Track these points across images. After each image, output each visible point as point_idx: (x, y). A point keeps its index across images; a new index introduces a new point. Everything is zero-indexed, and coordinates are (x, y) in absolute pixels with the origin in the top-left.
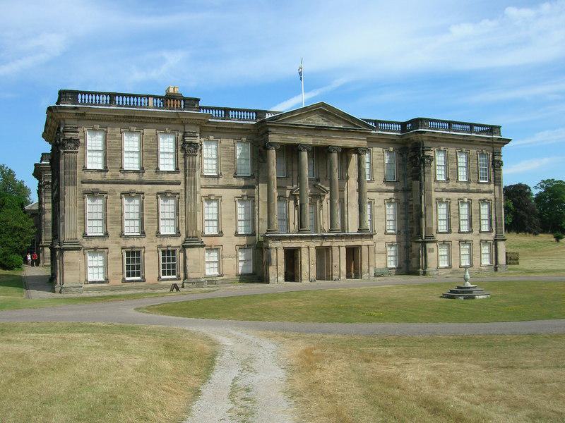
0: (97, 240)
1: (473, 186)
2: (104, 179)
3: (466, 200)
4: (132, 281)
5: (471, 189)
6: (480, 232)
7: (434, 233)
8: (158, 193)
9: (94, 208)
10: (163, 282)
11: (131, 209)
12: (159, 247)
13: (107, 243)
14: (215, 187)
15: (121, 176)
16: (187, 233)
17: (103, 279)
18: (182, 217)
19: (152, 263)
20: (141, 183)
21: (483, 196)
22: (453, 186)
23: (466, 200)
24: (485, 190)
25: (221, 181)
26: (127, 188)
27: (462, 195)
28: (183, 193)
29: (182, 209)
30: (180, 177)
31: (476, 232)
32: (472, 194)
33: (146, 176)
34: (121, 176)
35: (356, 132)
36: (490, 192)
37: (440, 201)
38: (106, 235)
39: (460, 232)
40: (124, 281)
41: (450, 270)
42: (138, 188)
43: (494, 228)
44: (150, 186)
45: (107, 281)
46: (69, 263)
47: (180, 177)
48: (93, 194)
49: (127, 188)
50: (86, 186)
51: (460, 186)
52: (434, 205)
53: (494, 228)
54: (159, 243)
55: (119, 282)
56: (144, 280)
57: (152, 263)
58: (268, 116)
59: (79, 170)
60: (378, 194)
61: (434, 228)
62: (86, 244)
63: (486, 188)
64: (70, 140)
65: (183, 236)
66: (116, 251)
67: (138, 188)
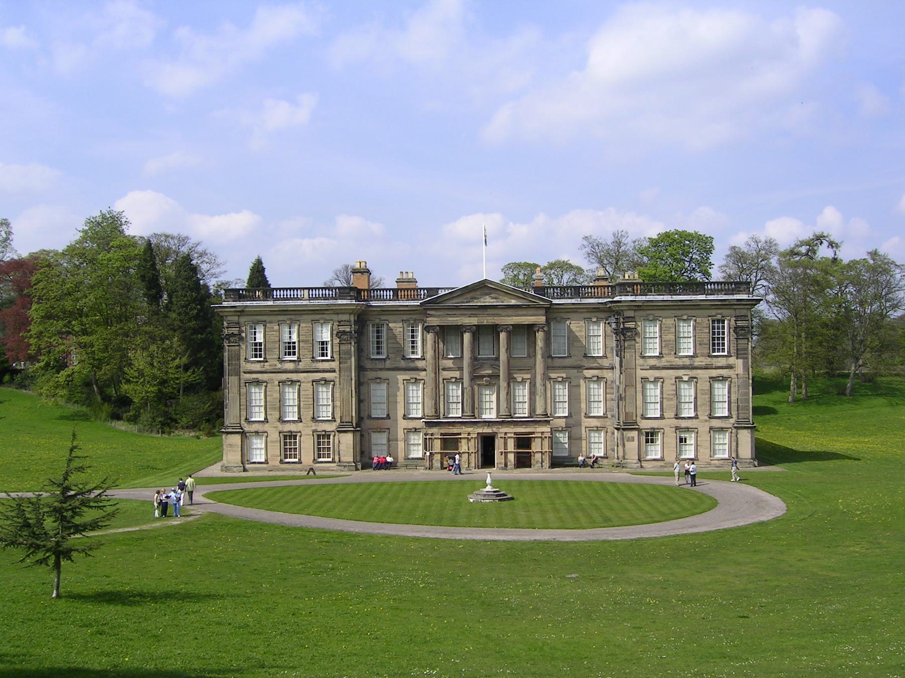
0: (256, 425)
1: (697, 362)
2: (263, 369)
3: (686, 378)
4: (289, 463)
5: (696, 364)
6: (711, 417)
7: (639, 419)
8: (313, 381)
9: (257, 395)
10: (318, 465)
11: (291, 395)
12: (314, 431)
13: (266, 427)
14: (381, 369)
15: (279, 366)
16: (341, 417)
17: (263, 460)
18: (338, 403)
19: (307, 446)
20: (296, 372)
21: (715, 373)
22: (668, 362)
23: (686, 378)
24: (720, 364)
25: (388, 364)
26: (284, 376)
27: (680, 373)
28: (338, 380)
29: (337, 395)
30: (335, 365)
31: (703, 416)
32: (699, 371)
33: (301, 366)
34: (279, 366)
35: (528, 307)
36: (730, 367)
37: (645, 380)
38: (267, 420)
39: (677, 417)
40: (281, 462)
41: (662, 463)
42: (294, 376)
43: (734, 413)
44: (305, 374)
45: (266, 462)
46: (231, 445)
47: (335, 365)
48: (258, 383)
49: (284, 376)
50: (248, 376)
51: (679, 362)
52: (639, 386)
53: (734, 413)
54: (314, 428)
55: (277, 463)
56: (300, 462)
57: (307, 446)
58: (441, 293)
59: (243, 363)
60: (576, 371)
61: (640, 412)
62: (247, 428)
63: (722, 362)
64: (233, 335)
65: (338, 420)
66: (274, 436)
67: (294, 376)
